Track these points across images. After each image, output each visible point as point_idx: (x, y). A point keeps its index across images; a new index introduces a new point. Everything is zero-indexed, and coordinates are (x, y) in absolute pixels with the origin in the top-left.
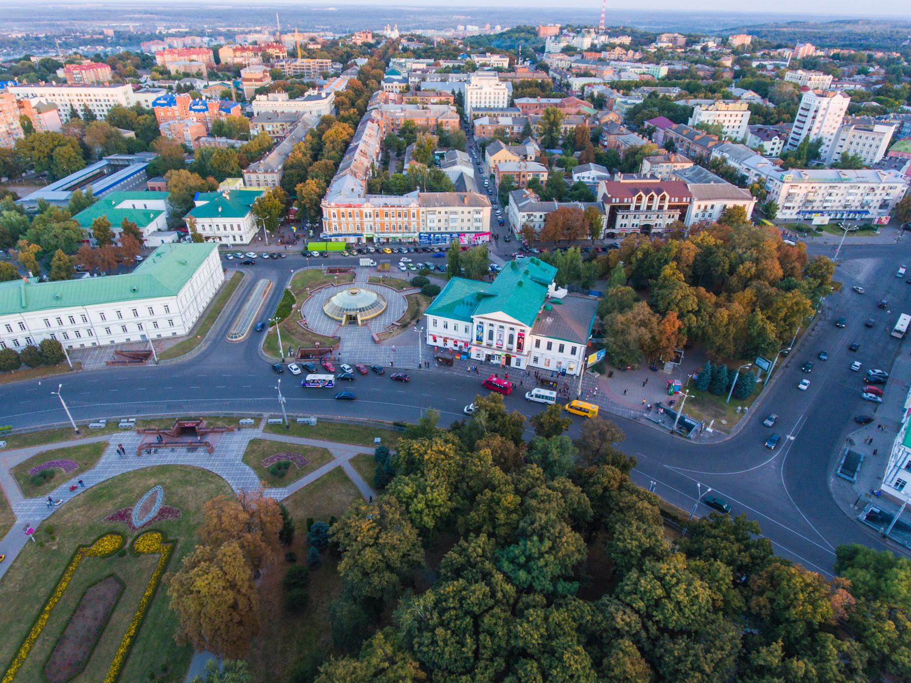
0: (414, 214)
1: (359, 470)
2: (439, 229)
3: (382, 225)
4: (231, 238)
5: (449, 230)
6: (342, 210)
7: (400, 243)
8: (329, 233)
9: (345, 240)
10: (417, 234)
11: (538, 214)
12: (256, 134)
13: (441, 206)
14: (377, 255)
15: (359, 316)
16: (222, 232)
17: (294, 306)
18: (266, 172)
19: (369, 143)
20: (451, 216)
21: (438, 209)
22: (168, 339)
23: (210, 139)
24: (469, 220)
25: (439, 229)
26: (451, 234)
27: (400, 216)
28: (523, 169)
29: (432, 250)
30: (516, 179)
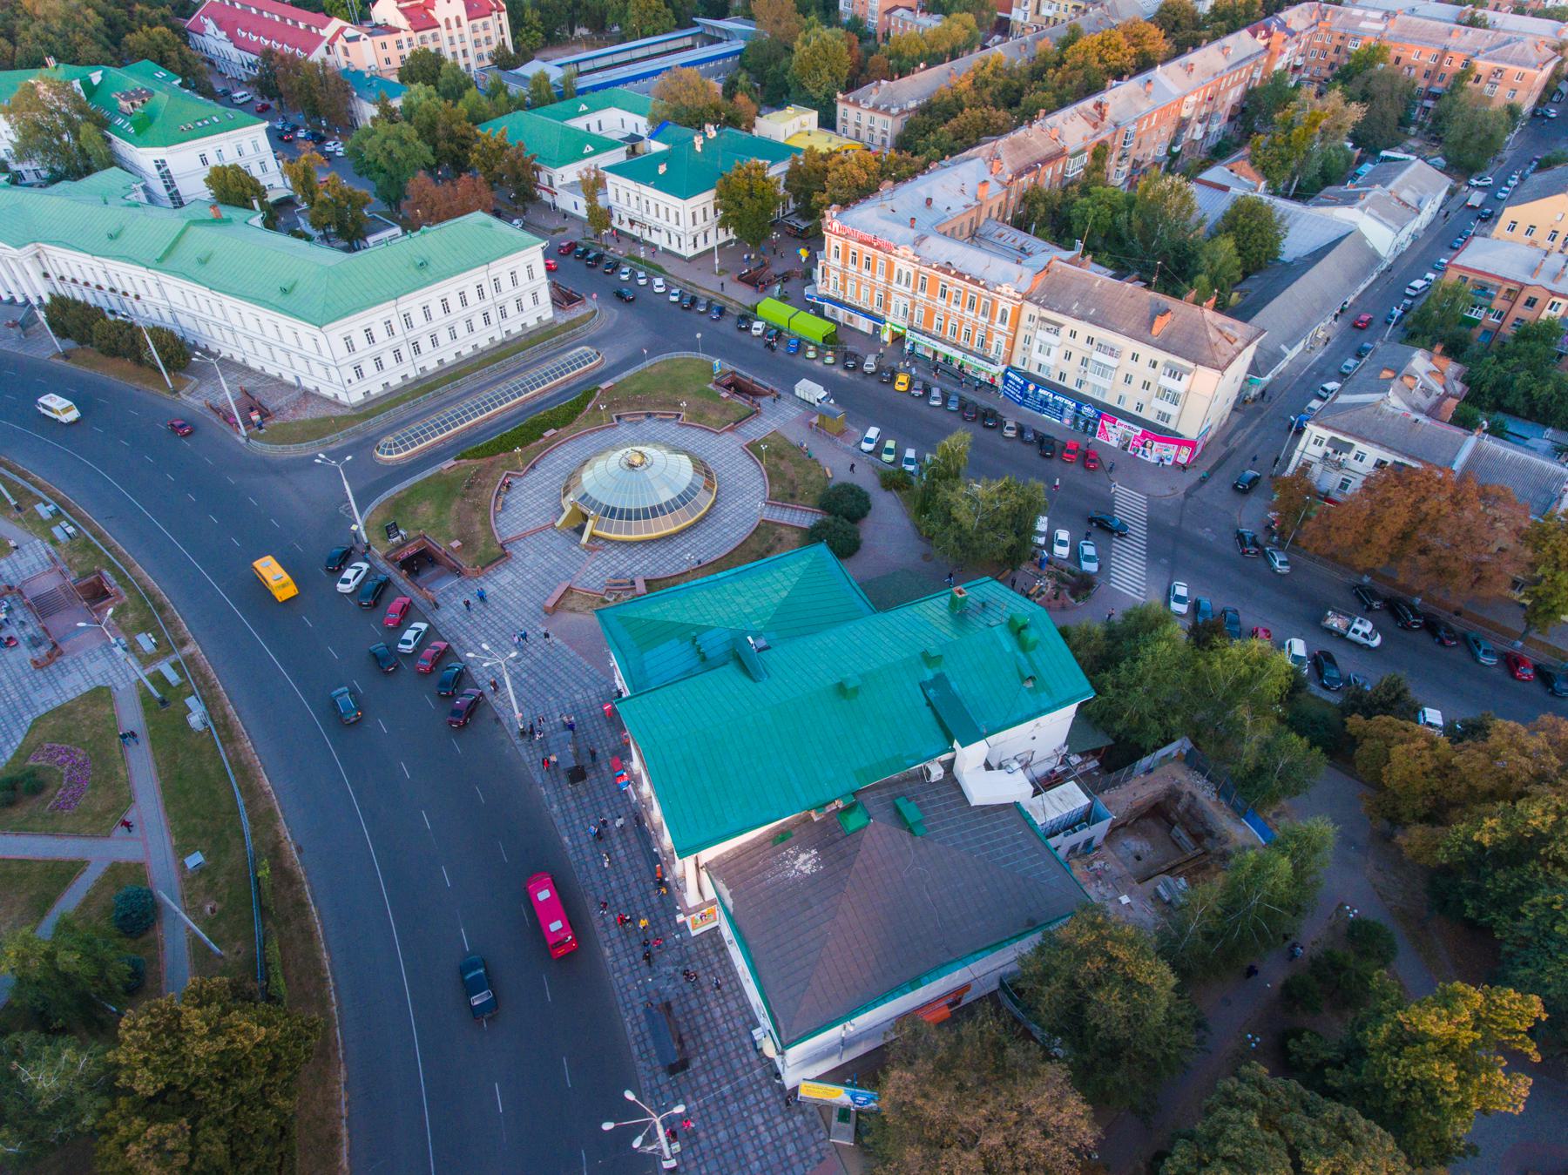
0: (1004, 311)
1: (86, 903)
2: (1062, 376)
3: (930, 313)
4: (664, 236)
5: (1086, 391)
6: (854, 246)
7: (960, 375)
8: (821, 288)
9: (850, 318)
10: (1002, 368)
11: (1373, 453)
12: (1021, 19)
13: (1081, 318)
14: (872, 384)
15: (590, 523)
16: (650, 218)
17: (553, 431)
18: (875, 108)
19: (1191, 88)
20: (1099, 357)
21: (1070, 323)
22: (326, 400)
23: (908, 15)
24: (1146, 385)
25: (1062, 376)
26: (1081, 400)
27: (971, 306)
28: (1542, 280)
29: (1000, 424)
30: (1499, 304)
